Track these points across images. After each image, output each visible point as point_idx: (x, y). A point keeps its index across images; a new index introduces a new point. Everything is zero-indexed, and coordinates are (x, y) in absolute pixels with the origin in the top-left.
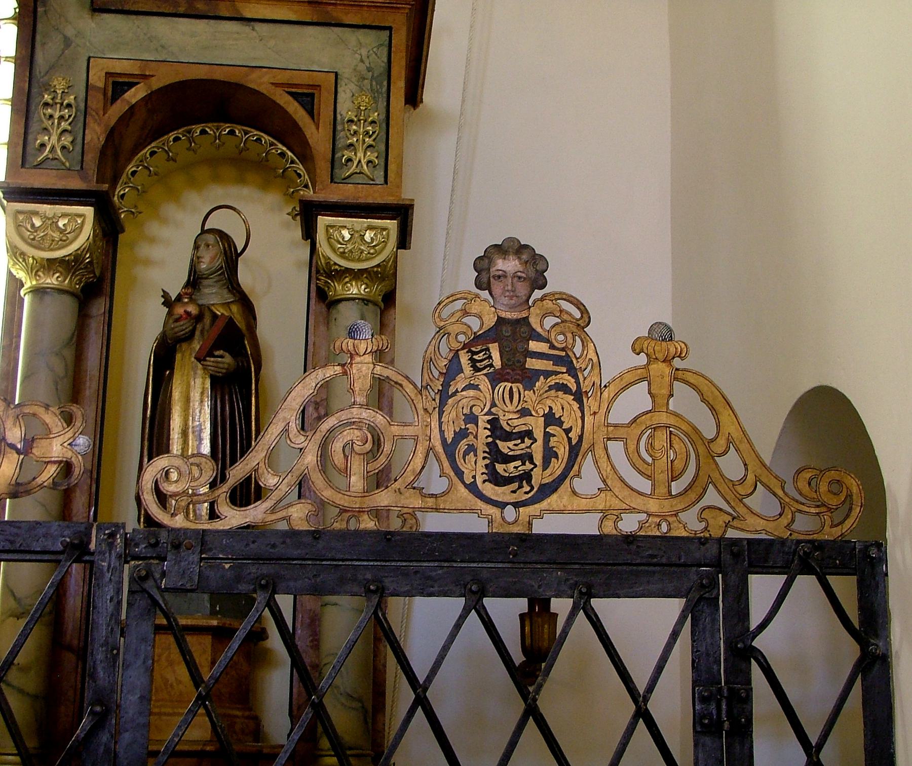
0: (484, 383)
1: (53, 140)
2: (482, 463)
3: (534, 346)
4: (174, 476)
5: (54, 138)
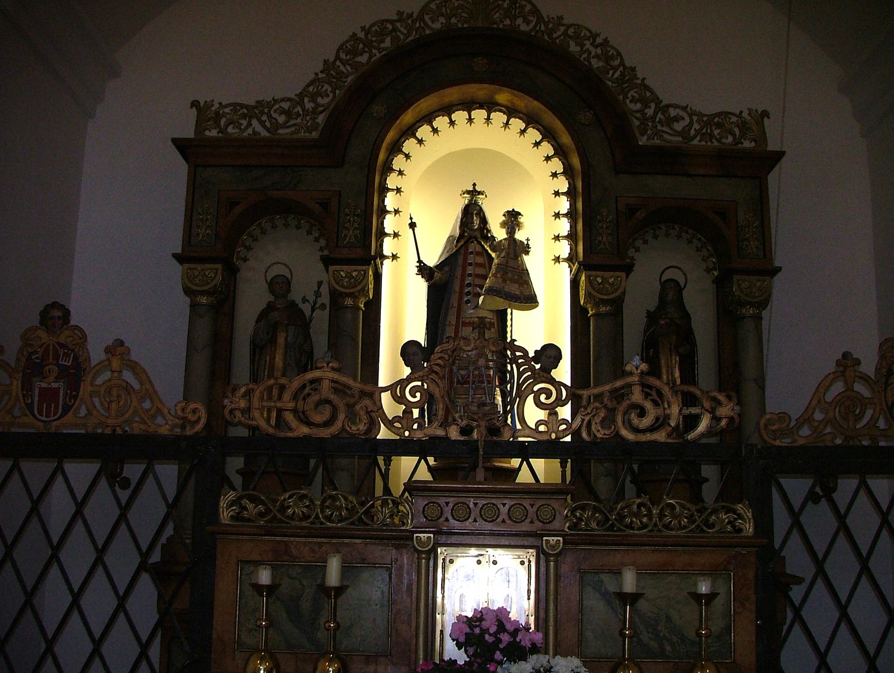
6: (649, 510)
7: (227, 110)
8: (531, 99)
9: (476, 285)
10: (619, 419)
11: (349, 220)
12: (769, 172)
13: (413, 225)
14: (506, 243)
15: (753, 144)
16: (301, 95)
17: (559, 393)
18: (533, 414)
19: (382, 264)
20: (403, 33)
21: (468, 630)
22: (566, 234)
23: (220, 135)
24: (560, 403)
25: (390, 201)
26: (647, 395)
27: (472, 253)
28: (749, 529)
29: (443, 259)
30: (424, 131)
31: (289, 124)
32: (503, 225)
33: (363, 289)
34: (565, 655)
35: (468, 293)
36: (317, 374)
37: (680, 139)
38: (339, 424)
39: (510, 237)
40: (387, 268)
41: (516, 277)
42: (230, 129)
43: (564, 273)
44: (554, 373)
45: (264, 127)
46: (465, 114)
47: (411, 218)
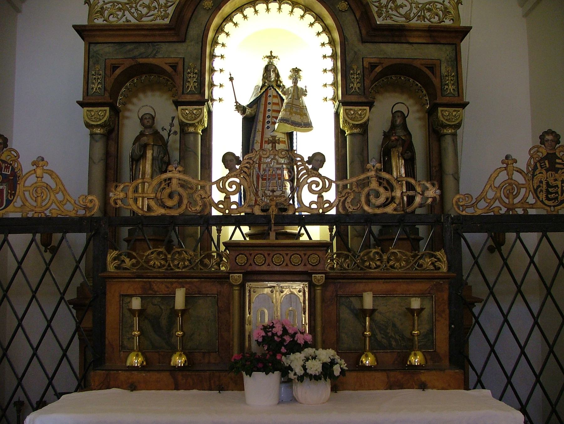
0: (544, 172)
1: (356, 85)
2: (544, 195)
3: (557, 161)
4: (461, 200)
5: (355, 85)
6: (381, 256)
7: (108, 6)
9: (273, 117)
11: (190, 77)
12: (461, 41)
13: (231, 79)
14: (292, 89)
17: (324, 184)
19: (212, 104)
21: (264, 334)
22: (331, 83)
24: (325, 190)
25: (217, 64)
26: (380, 184)
27: (270, 96)
28: (444, 268)
29: (252, 100)
30: (238, 18)
31: (148, 15)
32: (291, 77)
33: (201, 121)
34: (324, 348)
35: (268, 122)
36: (168, 175)
37: (404, 19)
38: (184, 207)
39: (294, 85)
40: (216, 108)
41: (299, 111)
43: (330, 108)
44: (321, 171)
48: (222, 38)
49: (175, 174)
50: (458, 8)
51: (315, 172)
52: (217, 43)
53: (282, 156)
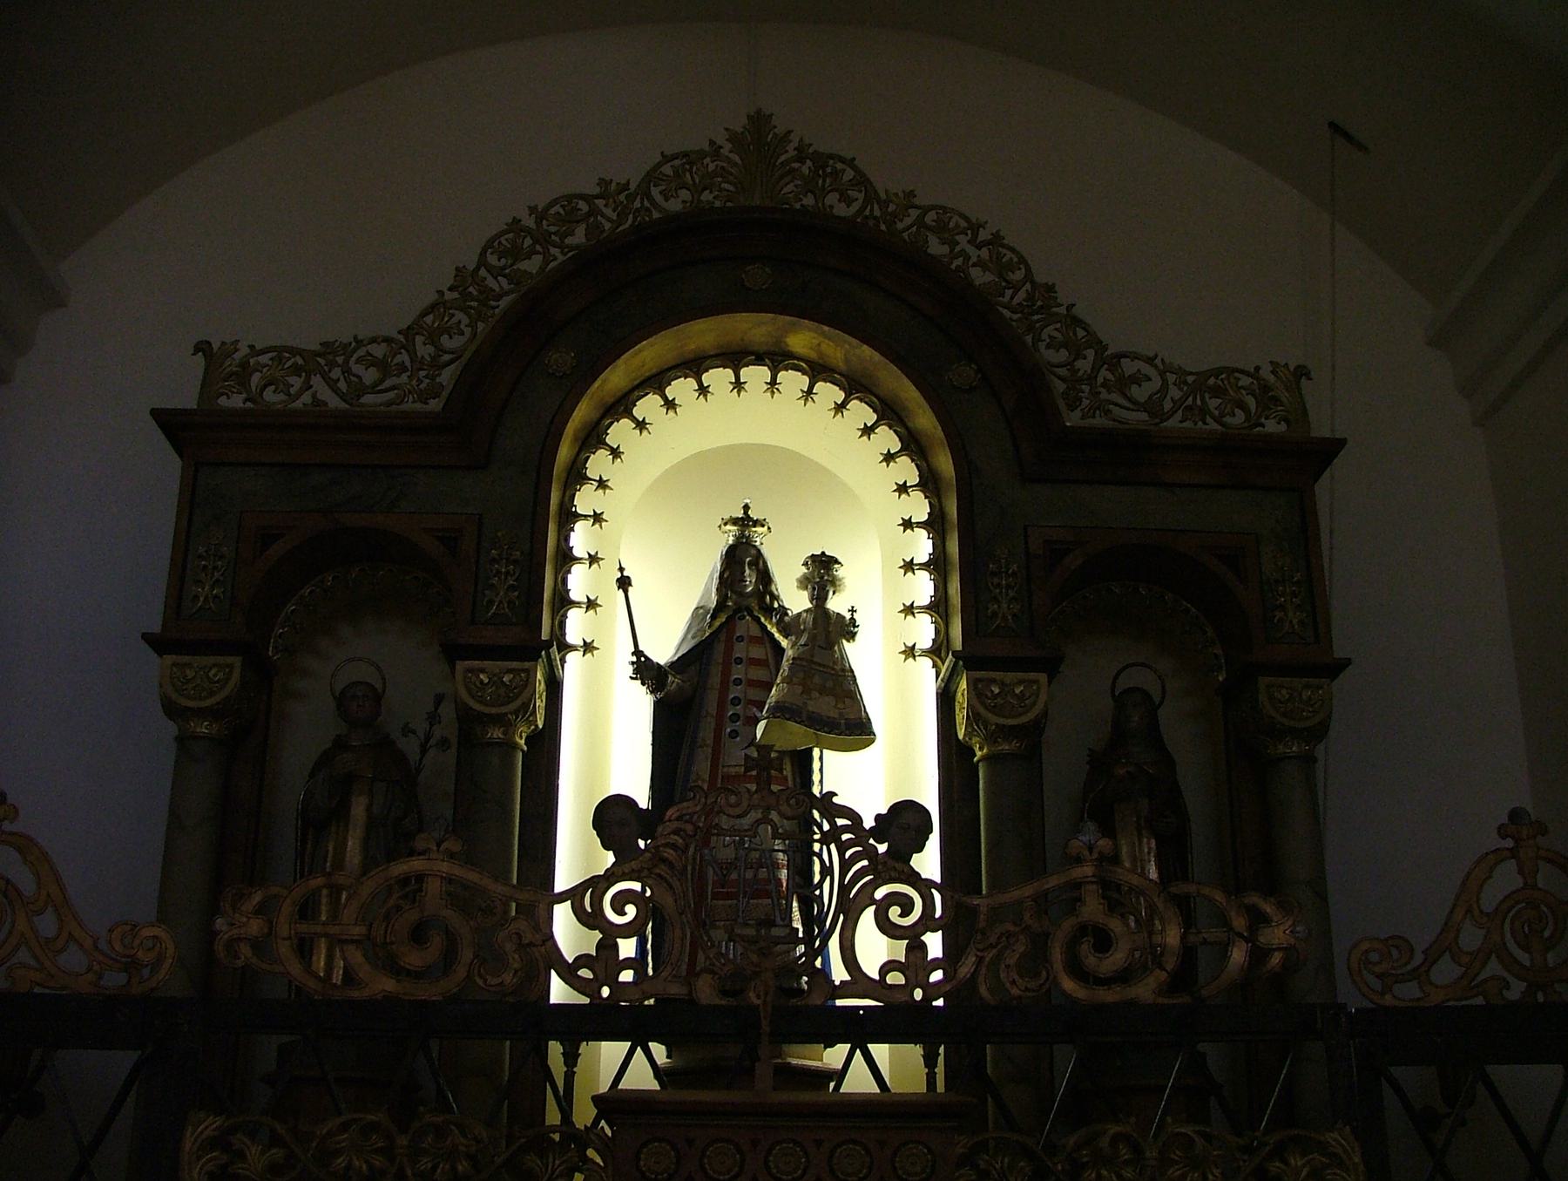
7: (264, 359)
8: (855, 342)
10: (1057, 955)
11: (498, 572)
12: (1316, 481)
14: (810, 618)
15: (1283, 427)
16: (409, 332)
18: (875, 949)
19: (563, 661)
20: (609, 220)
22: (926, 601)
23: (249, 404)
25: (581, 539)
27: (740, 639)
30: (648, 406)
32: (804, 582)
33: (525, 706)
36: (417, 864)
37: (1144, 416)
38: (461, 972)
39: (816, 607)
40: (574, 668)
42: (269, 395)
43: (924, 678)
45: (336, 391)
46: (728, 374)
47: (621, 569)
48: (598, 463)
49: (435, 864)
50: (1299, 389)
51: (899, 866)
52: (583, 479)
53: (789, 812)
